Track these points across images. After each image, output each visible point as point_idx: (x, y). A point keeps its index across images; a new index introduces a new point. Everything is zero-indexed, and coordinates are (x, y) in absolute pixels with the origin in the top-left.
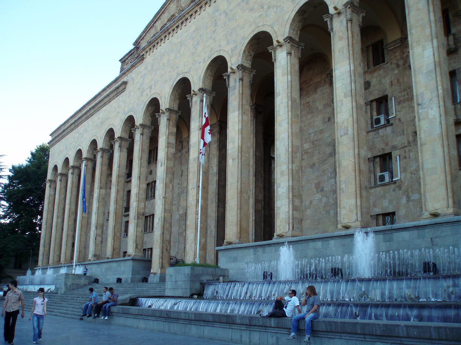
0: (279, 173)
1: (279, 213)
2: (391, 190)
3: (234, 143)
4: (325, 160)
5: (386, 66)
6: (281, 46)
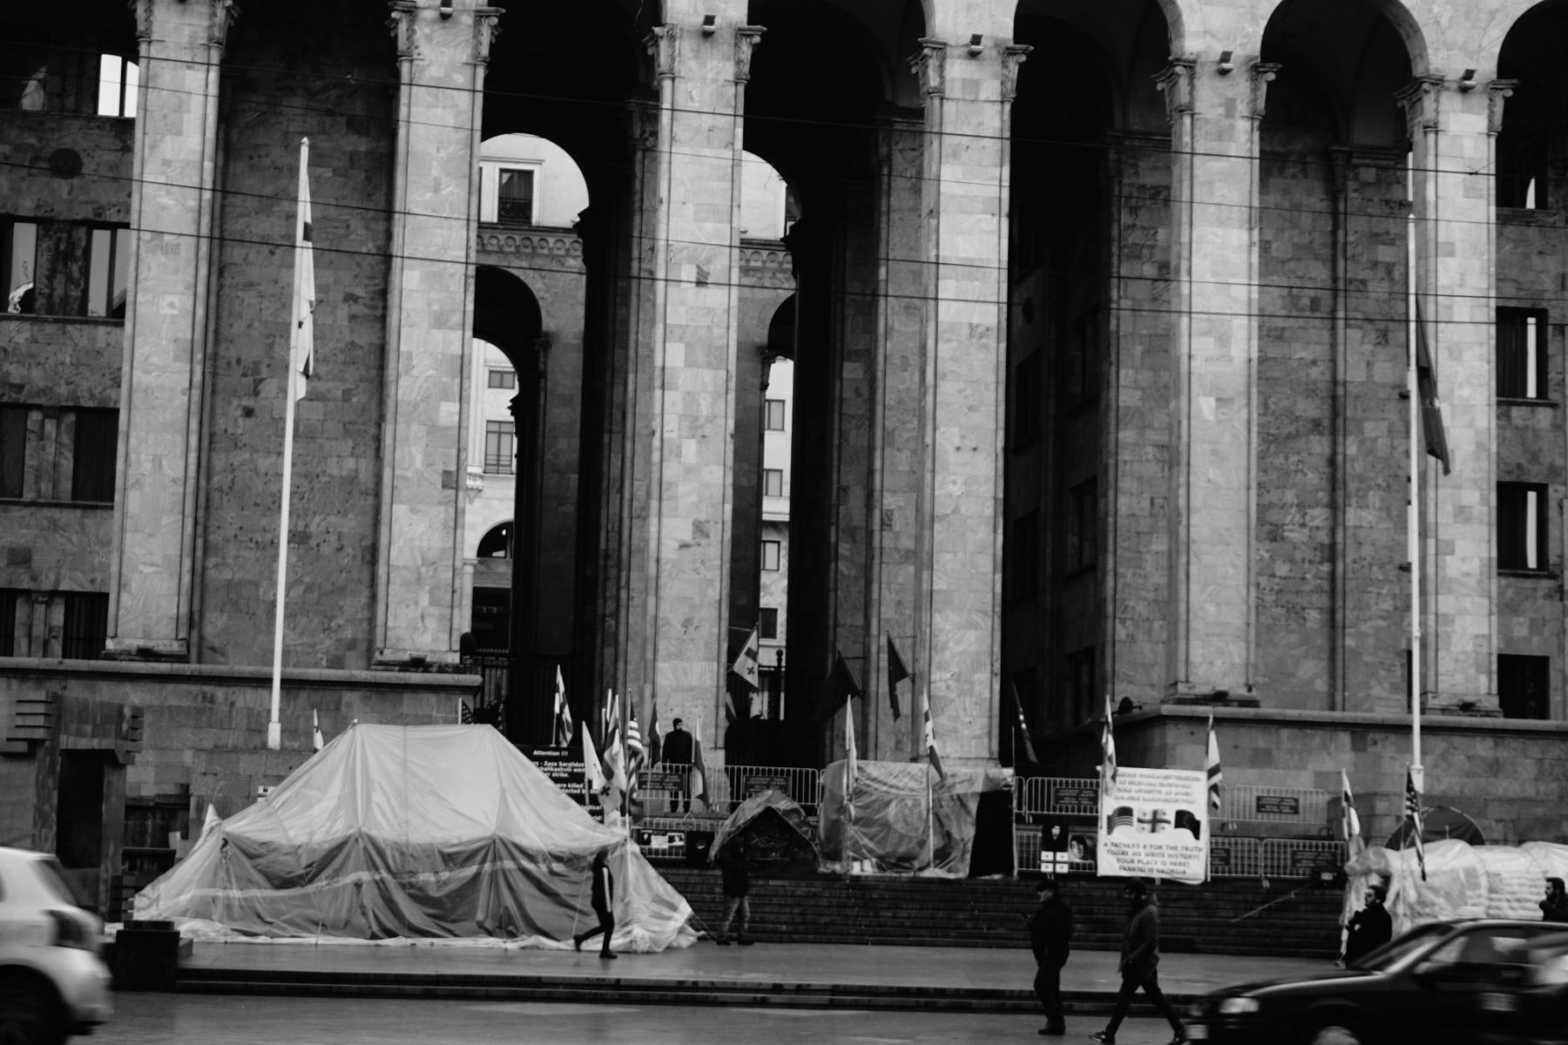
0: (1450, 508)
1: (1448, 634)
2: (1540, 594)
3: (1223, 340)
4: (1289, 437)
5: (1551, 220)
6: (1465, 90)
